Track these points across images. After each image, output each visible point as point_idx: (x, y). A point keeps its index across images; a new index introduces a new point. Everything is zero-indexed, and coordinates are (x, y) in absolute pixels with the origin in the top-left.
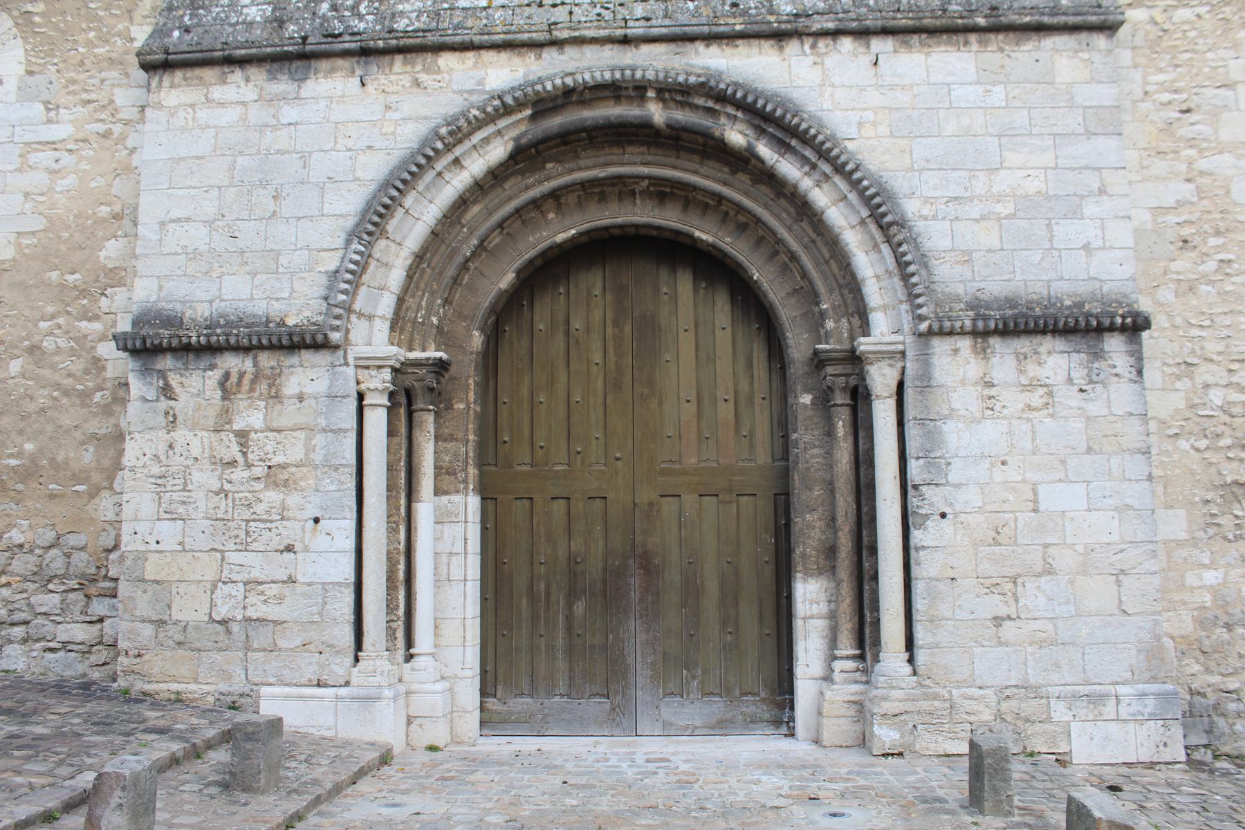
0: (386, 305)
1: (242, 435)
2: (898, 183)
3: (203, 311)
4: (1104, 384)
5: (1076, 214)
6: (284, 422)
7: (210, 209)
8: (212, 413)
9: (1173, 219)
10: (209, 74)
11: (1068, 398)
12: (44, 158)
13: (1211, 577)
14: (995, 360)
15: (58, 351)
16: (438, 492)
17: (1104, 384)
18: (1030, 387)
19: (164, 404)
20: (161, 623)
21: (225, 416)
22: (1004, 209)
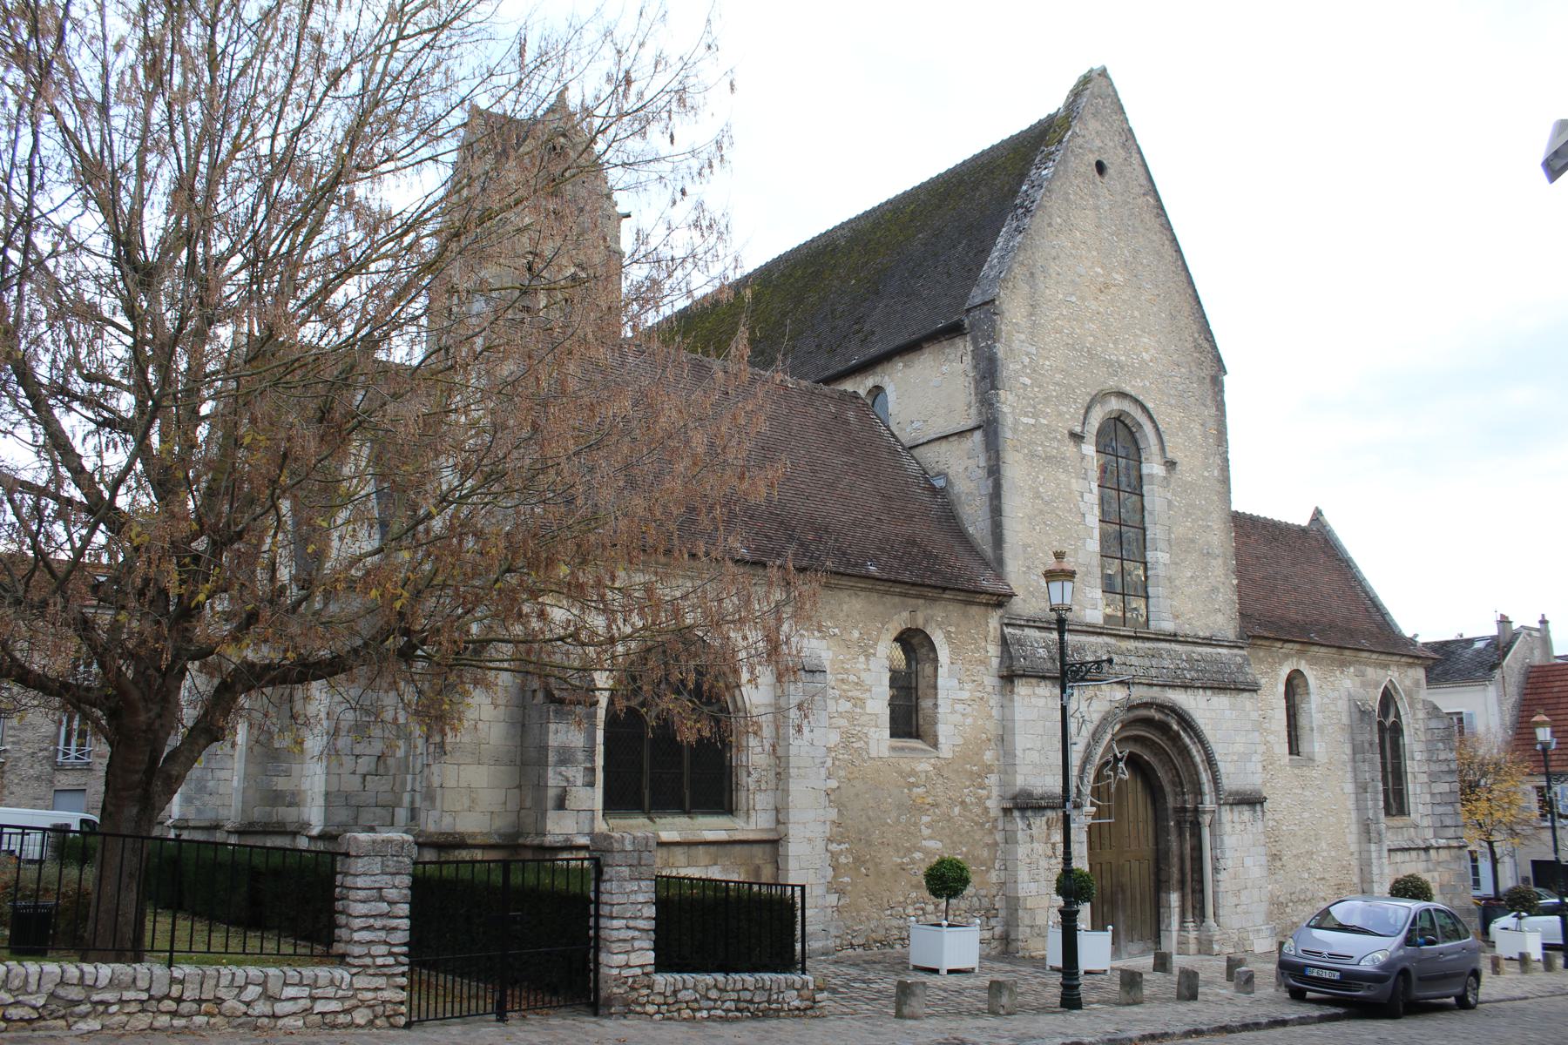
7: (1039, 745)
8: (1044, 835)
10: (1034, 681)
12: (959, 707)
19: (1029, 832)
20: (1032, 927)
22: (1235, 758)
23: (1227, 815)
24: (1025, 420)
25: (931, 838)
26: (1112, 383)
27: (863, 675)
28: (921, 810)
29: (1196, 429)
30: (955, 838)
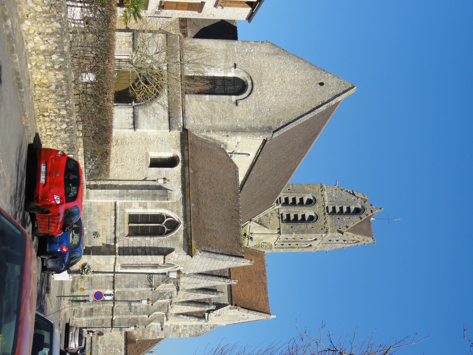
1: (125, 44)
4: (129, 125)
5: (148, 124)
9: (149, 138)
11: (127, 121)
14: (131, 114)
15: (135, 26)
17: (129, 125)
18: (128, 118)
19: (128, 36)
21: (127, 42)
23: (131, 110)
24: (235, 49)
26: (255, 82)
29: (251, 117)
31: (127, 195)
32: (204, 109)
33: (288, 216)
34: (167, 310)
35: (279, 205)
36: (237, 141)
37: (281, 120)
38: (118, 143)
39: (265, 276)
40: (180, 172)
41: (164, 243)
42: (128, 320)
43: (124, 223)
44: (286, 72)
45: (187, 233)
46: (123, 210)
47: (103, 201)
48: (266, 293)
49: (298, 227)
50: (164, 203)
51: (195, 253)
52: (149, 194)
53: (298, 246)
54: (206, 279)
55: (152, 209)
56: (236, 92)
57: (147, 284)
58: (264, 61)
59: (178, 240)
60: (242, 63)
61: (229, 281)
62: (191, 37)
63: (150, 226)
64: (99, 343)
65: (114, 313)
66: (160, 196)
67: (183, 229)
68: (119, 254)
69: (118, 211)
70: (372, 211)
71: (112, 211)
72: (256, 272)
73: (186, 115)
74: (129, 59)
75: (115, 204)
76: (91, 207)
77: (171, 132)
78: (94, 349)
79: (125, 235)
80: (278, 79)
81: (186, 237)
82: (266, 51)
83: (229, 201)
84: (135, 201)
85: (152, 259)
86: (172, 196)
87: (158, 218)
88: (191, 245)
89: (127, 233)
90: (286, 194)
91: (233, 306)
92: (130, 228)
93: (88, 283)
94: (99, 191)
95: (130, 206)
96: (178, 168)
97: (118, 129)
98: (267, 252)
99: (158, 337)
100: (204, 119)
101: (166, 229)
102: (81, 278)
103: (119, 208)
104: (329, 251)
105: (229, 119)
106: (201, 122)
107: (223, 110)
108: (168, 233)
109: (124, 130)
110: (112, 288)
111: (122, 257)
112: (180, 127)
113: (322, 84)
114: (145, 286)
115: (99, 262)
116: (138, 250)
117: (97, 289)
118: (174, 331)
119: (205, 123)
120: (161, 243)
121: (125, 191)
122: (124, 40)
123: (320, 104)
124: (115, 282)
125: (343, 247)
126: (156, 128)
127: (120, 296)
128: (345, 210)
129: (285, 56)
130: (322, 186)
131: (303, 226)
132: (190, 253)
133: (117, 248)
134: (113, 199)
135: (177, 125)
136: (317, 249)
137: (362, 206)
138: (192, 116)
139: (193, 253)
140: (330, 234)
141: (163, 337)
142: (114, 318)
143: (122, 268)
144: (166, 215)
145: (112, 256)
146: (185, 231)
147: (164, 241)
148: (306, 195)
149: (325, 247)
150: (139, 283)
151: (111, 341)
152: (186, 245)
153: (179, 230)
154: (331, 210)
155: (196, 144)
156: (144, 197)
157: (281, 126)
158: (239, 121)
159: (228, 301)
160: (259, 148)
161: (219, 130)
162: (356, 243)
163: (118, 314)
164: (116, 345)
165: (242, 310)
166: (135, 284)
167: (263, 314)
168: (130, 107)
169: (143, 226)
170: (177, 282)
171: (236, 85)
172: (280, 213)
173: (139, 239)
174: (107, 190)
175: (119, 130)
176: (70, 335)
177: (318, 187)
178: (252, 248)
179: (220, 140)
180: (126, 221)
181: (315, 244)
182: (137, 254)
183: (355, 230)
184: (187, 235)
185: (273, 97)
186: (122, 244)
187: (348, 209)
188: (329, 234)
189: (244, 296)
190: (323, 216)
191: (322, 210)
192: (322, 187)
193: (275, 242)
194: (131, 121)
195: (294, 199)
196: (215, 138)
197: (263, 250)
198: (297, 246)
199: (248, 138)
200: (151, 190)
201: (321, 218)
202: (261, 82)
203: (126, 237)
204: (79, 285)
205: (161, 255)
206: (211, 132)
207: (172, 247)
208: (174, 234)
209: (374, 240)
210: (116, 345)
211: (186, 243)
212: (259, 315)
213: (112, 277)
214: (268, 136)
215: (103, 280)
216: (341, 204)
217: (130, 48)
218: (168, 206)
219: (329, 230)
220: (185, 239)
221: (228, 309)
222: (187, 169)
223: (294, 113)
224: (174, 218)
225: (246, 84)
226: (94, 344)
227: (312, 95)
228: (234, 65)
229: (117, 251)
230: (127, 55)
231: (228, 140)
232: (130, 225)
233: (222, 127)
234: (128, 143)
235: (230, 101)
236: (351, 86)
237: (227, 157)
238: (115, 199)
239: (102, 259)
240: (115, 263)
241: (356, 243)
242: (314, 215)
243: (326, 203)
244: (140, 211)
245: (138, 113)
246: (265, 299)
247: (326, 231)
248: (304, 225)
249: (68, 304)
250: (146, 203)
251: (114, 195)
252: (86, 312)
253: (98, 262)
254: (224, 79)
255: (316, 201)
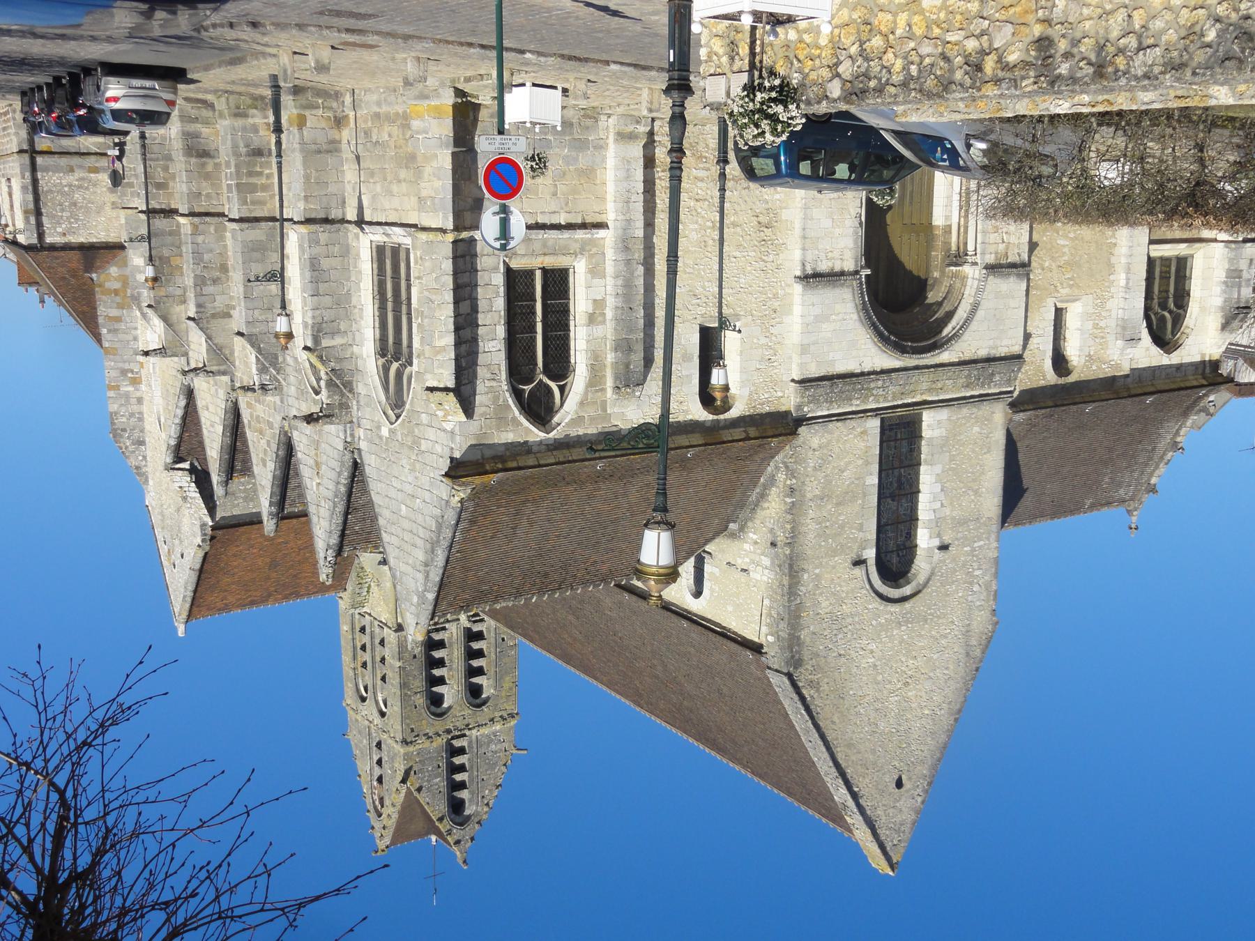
0: (969, 282)
1: (1003, 242)
2: (858, 325)
3: (1012, 279)
5: (816, 316)
6: (995, 246)
11: (822, 256)
13: (777, 196)
16: (950, 226)
21: (1007, 248)
23: (849, 266)
24: (982, 543)
25: (1064, 246)
26: (907, 605)
27: (1092, 343)
28: (1067, 263)
29: (825, 605)
30: (1049, 246)
31: (628, 262)
32: (845, 474)
33: (441, 644)
34: (211, 372)
35: (469, 621)
36: (751, 568)
37: (818, 690)
38: (765, 230)
39: (286, 597)
40: (689, 417)
41: (488, 384)
42: (168, 258)
43: (545, 254)
44: (928, 685)
45: (518, 455)
46: (582, 251)
47: (611, 188)
48: (243, 606)
49: (416, 673)
50: (605, 376)
51: (464, 484)
52: (631, 331)
53: (360, 669)
54: (336, 496)
55: (588, 341)
56: (883, 555)
57: (324, 325)
58: (952, 622)
59: (498, 428)
60: (950, 566)
61: (329, 559)
62: (1011, 420)
63: (535, 337)
64: (79, 174)
65: (196, 220)
66: (627, 366)
67: (531, 439)
68: (455, 242)
69: (580, 234)
70: (458, 842)
71: (580, 215)
72: (295, 576)
73: (831, 425)
74: (967, 255)
75: (601, 225)
76: (591, 149)
77: (793, 384)
78: (64, 161)
79: (510, 258)
80: (912, 666)
81: (508, 453)
82: (975, 623)
83: (591, 560)
84: (609, 288)
85: (443, 349)
86: (626, 402)
87: (559, 365)
88: (486, 473)
89: (515, 264)
90: (493, 634)
91: (209, 531)
92: (530, 274)
93: (321, 139)
94: (639, 174)
95: (596, 271)
96: (698, 413)
97: (804, 229)
98: (346, 595)
99: (104, 331)
100: (820, 475)
101: (527, 388)
102: (335, 117)
103: (589, 236)
104: (349, 740)
105: (820, 546)
106: (815, 469)
107: (842, 527)
108: (517, 394)
109: (799, 246)
110: (308, 217)
111: (448, 250)
112: (806, 409)
113: (899, 784)
114: (319, 320)
115: (426, 175)
116: (468, 302)
117: (305, 170)
118: (124, 372)
119: (812, 479)
120: (489, 376)
121: (639, 255)
122: (1013, 239)
123: (856, 789)
124: (328, 226)
125: (360, 776)
126: (806, 342)
127: (264, 238)
128: (458, 777)
129: (962, 678)
130: (513, 717)
131: (419, 683)
132: (457, 470)
133: (472, 233)
134: (619, 218)
135: (809, 402)
136: (351, 713)
137: (469, 817)
138: (829, 442)
139: (464, 480)
140: (402, 751)
141: (106, 344)
142: (182, 220)
143: (374, 246)
144: (569, 385)
145: (451, 219)
146: (524, 449)
147: (494, 384)
148: (491, 682)
149: (360, 732)
150: (327, 300)
151: (86, 207)
152: (483, 455)
153: (527, 428)
154: (457, 743)
155: (756, 458)
156: (622, 314)
157: (804, 691)
158: (817, 575)
159: (223, 518)
160: (724, 628)
161: (794, 521)
162: (375, 807)
163: (196, 231)
164: (77, 220)
165: (201, 554)
166: (323, 287)
167: (188, 605)
168: (856, 261)
169: (534, 313)
170: (333, 416)
171: (898, 555)
172: (447, 625)
173: (500, 303)
174: (641, 197)
175: (797, 231)
176: (148, 83)
177: (511, 707)
178: (356, 562)
179: (758, 522)
180: (550, 262)
181: (369, 710)
182: (457, 302)
183: (411, 808)
184: (514, 456)
185: (872, 660)
186: (482, 251)
187: (462, 785)
188: (400, 750)
189: (235, 555)
190: (443, 729)
191: (458, 724)
192: (512, 716)
193: (370, 615)
194: (824, 267)
195: (479, 654)
196: (763, 509)
197: (349, 587)
198: (360, 664)
199: (767, 602)
200: (642, 334)
201: (440, 725)
202: (907, 622)
203: (504, 261)
204: (314, 112)
205: (456, 378)
206: (789, 500)
207: (478, 410)
208: (517, 413)
209: (383, 851)
210: (77, 220)
211: (488, 453)
212: (185, 597)
213: (340, 217)
214: (774, 656)
215: (332, 189)
216: (472, 767)
217: (993, 255)
218: (597, 391)
219: (411, 749)
220: (503, 449)
221: (201, 518)
222: (697, 439)
223: (833, 723)
224: (562, 411)
225: (901, 581)
226: (76, 161)
227: (875, 763)
228: (946, 543)
229: (464, 235)
230: (976, 250)
231: (756, 543)
232: (538, 274)
233: (803, 529)
234: (764, 261)
235: (864, 544)
236: (895, 861)
237: (702, 540)
238: (618, 224)
239: (438, 184)
240: (424, 229)
241: (375, 807)
242: (445, 705)
243: (474, 732)
244: (580, 303)
245: (842, 285)
246: (226, 605)
247: (409, 740)
248: (419, 684)
249: (317, 62)
250: (604, 322)
251: (629, 221)
252: (196, 135)
253: (428, 170)
254: (912, 519)
255: (479, 706)
